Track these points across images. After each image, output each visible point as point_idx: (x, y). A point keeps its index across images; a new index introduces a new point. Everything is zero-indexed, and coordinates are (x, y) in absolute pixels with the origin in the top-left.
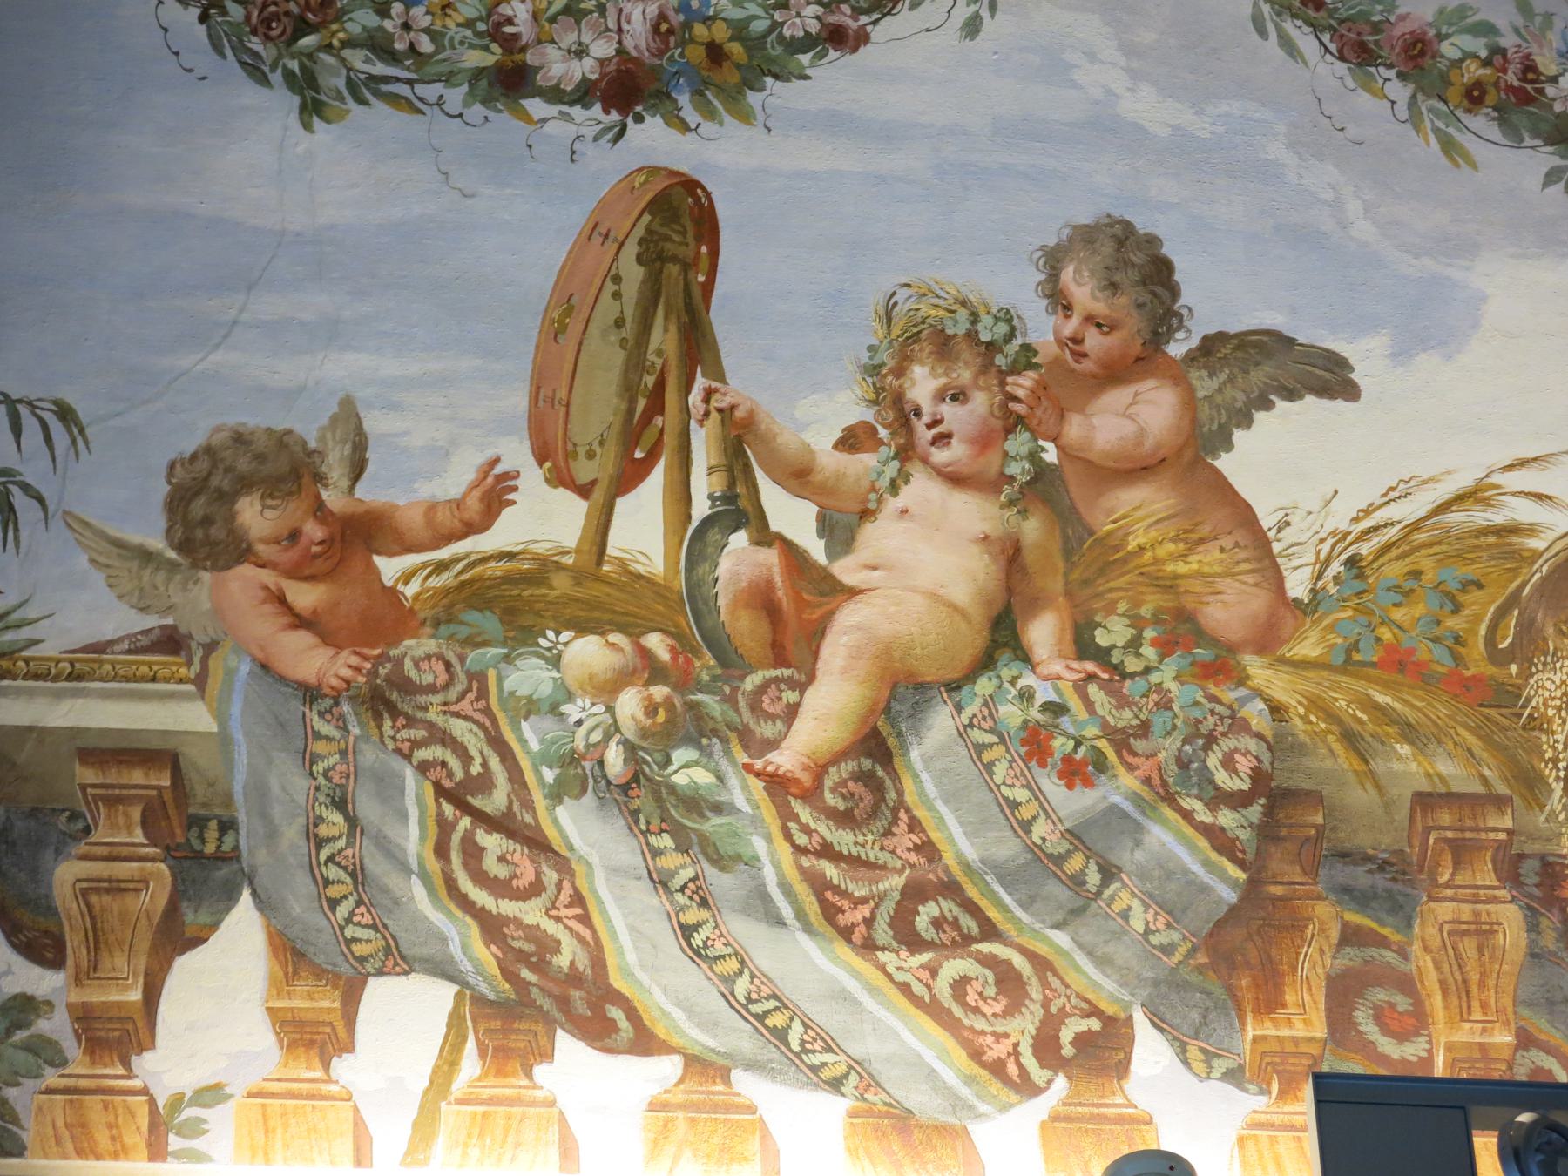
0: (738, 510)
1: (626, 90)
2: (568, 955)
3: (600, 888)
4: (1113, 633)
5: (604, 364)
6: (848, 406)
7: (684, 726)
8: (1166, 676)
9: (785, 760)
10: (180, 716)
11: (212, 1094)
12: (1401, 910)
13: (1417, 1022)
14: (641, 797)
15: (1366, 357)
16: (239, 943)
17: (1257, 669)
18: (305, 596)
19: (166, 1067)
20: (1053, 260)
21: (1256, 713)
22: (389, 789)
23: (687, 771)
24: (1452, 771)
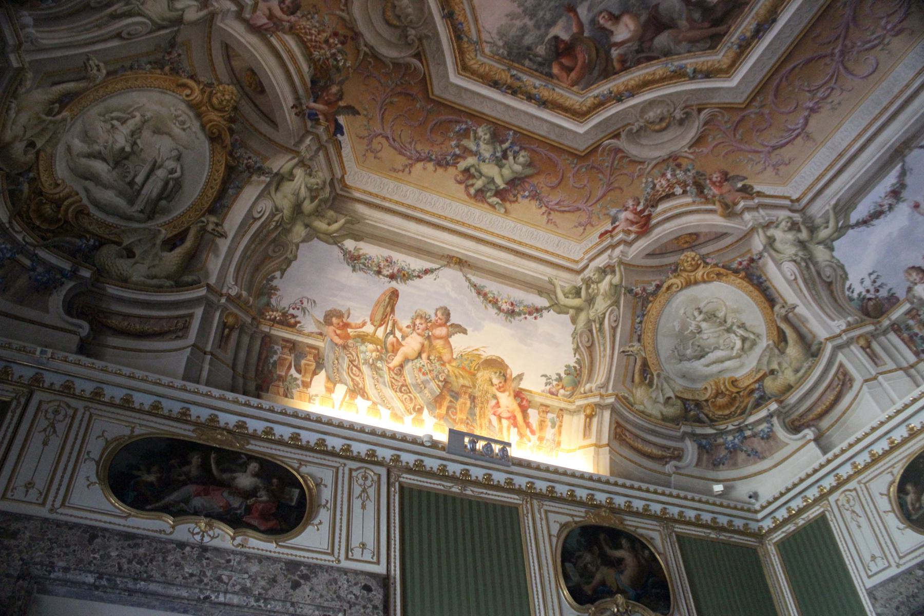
0: (392, 332)
1: (392, 277)
2: (361, 386)
3: (366, 378)
4: (432, 358)
5: (381, 310)
6: (409, 322)
7: (380, 359)
8: (437, 364)
9: (391, 365)
10: (320, 344)
11: (316, 395)
12: (457, 399)
13: (455, 414)
14: (373, 366)
15: (469, 330)
16: (322, 375)
17: (448, 366)
18: (338, 332)
19: (312, 390)
20: (437, 310)
21: (446, 371)
22: (343, 359)
23: (379, 364)
24: (467, 383)
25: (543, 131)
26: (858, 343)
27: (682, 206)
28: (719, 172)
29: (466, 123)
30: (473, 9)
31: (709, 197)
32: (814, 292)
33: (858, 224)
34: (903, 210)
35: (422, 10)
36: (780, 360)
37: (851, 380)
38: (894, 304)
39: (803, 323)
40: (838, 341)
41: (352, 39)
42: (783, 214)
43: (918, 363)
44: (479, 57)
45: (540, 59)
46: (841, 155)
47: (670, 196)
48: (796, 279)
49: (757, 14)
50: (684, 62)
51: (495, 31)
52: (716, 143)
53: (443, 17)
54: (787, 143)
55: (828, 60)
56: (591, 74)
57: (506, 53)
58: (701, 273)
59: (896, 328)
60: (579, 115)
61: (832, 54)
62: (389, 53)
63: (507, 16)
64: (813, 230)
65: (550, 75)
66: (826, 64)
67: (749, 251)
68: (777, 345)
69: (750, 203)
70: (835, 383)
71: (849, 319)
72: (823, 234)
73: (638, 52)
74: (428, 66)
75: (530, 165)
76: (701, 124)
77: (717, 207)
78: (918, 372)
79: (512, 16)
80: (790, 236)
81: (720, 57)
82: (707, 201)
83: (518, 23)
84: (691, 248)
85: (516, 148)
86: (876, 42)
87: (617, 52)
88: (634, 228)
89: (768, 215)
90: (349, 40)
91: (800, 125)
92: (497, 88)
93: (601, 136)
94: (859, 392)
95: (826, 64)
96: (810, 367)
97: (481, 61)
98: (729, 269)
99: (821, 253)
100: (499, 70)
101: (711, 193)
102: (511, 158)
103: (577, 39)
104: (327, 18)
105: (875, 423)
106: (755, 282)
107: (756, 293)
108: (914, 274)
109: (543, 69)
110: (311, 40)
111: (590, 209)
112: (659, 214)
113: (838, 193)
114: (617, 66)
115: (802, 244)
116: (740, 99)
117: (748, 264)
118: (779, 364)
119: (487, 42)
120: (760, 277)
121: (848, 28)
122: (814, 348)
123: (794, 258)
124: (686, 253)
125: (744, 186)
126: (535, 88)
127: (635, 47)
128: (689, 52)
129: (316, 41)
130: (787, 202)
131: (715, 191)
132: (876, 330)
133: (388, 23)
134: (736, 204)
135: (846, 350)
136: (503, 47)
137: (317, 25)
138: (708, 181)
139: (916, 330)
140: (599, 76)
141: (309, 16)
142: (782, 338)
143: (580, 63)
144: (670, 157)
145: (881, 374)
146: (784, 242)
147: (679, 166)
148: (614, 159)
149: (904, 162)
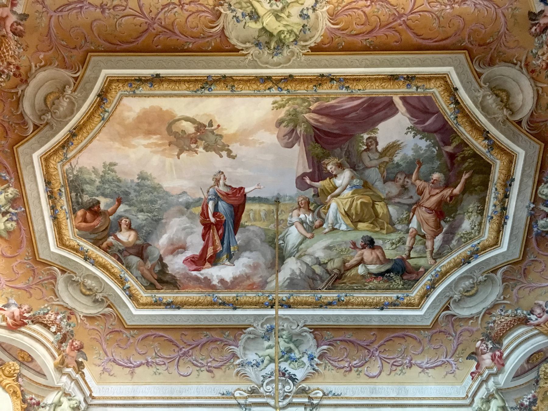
25: (37, 227)
27: (45, 338)
29: (11, 178)
30: (86, 146)
31: (62, 349)
35: (66, 117)
41: (21, 80)
44: (59, 165)
45: (80, 200)
46: (134, 398)
47: (46, 326)
49: (176, 297)
50: (130, 279)
51: (81, 166)
52: (96, 328)
53: (70, 131)
55: (177, 349)
56: (90, 234)
57: (72, 178)
58: (8, 382)
60: (61, 241)
61: (181, 349)
62: (26, 106)
63: (94, 168)
65: (74, 212)
67: (43, 397)
69: (74, 374)
73: (119, 251)
74: (33, 136)
75: (9, 232)
77: (58, 358)
79: (95, 171)
81: (144, 295)
82: (59, 350)
83: (93, 176)
84: (22, 364)
85: (15, 218)
86: (199, 365)
87: (112, 240)
88: (10, 321)
90: (19, 79)
91: (135, 364)
92: (46, 186)
93: (57, 263)
95: (174, 350)
97: (58, 169)
100: (58, 181)
101: (65, 348)
102: (6, 218)
103: (105, 214)
104: (24, 58)
109: (76, 206)
110: (4, 53)
111: (4, 286)
112: (30, 329)
114: (104, 245)
116: (130, 322)
117: (34, 404)
119: (71, 164)
121: (198, 346)
124: (15, 363)
125: (82, 362)
126: (61, 208)
127: (121, 248)
128: (137, 278)
129: (5, 57)
130: (88, 393)
131: (68, 349)
133: (45, 99)
134: (67, 367)
136: (74, 175)
137: (17, 53)
138: (71, 341)
140: (91, 239)
141: (19, 46)
143: (92, 224)
144: (70, 310)
147: (69, 318)
148: (48, 279)
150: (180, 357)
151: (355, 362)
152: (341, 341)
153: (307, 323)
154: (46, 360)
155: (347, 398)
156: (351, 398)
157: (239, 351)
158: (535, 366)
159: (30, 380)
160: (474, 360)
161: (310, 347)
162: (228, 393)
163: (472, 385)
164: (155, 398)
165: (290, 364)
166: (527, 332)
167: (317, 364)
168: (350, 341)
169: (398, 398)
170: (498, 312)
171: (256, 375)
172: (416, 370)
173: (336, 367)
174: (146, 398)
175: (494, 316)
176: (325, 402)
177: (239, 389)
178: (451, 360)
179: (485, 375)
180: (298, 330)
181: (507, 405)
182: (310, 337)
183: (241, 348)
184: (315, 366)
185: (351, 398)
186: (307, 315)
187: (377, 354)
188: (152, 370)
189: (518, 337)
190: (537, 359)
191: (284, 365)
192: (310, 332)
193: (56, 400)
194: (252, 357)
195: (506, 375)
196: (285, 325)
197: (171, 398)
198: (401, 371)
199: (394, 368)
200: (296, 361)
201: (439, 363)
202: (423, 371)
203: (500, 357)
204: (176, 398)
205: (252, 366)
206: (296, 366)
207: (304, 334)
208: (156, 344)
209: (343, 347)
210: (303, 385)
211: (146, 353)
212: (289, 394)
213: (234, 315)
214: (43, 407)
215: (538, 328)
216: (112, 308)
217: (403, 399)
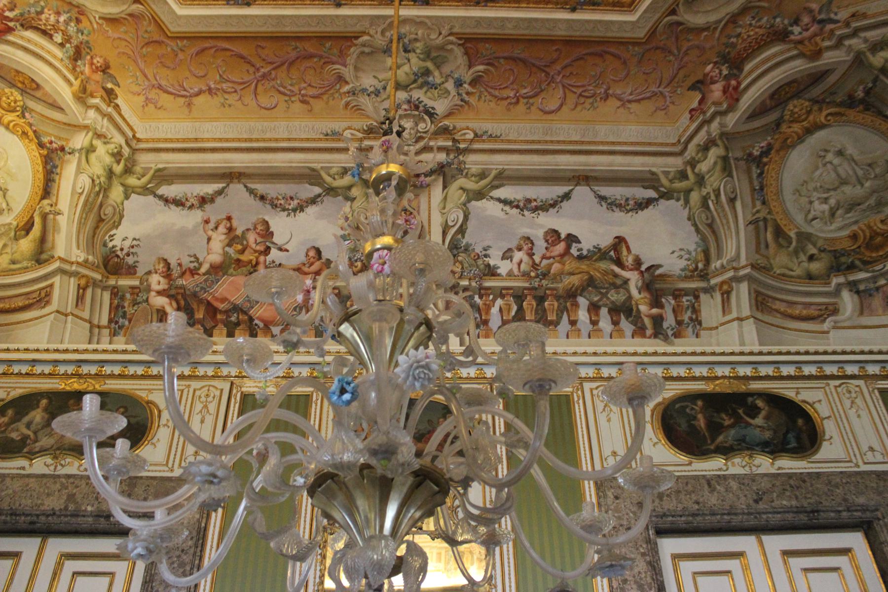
26: (79, 279)
27: (49, 52)
28: (105, 60)
31: (78, 70)
32: (84, 215)
33: (161, 197)
34: (197, 216)
36: (10, 243)
37: (48, 303)
38: (130, 274)
39: (54, 230)
40: (67, 267)
42: (119, 139)
43: (105, 327)
46: (196, 140)
48: (81, 194)
52: (123, 36)
54: (171, 93)
55: (252, 70)
59: (115, 292)
61: (258, 70)
64: (128, 171)
66: (248, 71)
67: (67, 140)
68: (17, 230)
69: (103, 106)
70: (34, 295)
71: (91, 258)
72: (132, 181)
76: (128, 11)
77: (77, 83)
78: (99, 334)
80: (108, 160)
82: (74, 70)
86: (288, 93)
89: (108, 129)
91: (192, 91)
94: (45, 316)
95: (248, 71)
96: (27, 268)
98: (37, 138)
99: (117, 193)
101: (82, 68)
105: (32, 346)
106: (49, 167)
107: (41, 176)
108: (162, 265)
113: (168, 163)
115: (110, 173)
116: (174, 28)
117: (56, 149)
118: (5, 246)
120: (56, 167)
121: (282, 64)
122: (44, 256)
123: (95, 178)
125: (112, 90)
130: (130, 134)
131: (87, 70)
132: (101, 281)
134: (92, 96)
135: (66, 278)
139: (126, 304)
142: (28, 227)
144: (78, 7)
145: (73, 315)
146: (99, 159)
147: (78, 21)
149: (228, 185)
150: (258, 81)
151: (525, 91)
152: (505, 58)
153: (455, 30)
154: (59, 85)
155: (509, 141)
156: (515, 142)
157: (347, 72)
158: (781, 104)
159: (43, 116)
160: (697, 92)
161: (458, 67)
162: (334, 133)
163: (688, 126)
164: (227, 140)
165: (426, 92)
166: (782, 53)
167: (468, 93)
168: (521, 60)
169: (582, 143)
170: (747, 20)
171: (375, 107)
172: (613, 103)
173: (496, 97)
174: (215, 140)
175: (740, 26)
176: (476, 146)
177: (349, 128)
178: (666, 92)
179: (708, 114)
180: (440, 41)
181: (730, 155)
182: (458, 52)
183: (351, 67)
184: (464, 95)
185: (515, 142)
186: (455, 17)
187: (558, 79)
188: (217, 100)
189: (768, 59)
190: (786, 93)
191: (417, 94)
192: (459, 45)
193: (86, 143)
194: (368, 81)
195: (738, 114)
196: (420, 32)
197: (251, 140)
198: (592, 104)
199: (582, 100)
200: (436, 88)
201: (648, 95)
202: (623, 105)
203: (736, 89)
204: (257, 140)
205: (369, 95)
206: (436, 95)
207: (450, 47)
208: (219, 61)
209: (508, 67)
210: (447, 122)
211: (204, 77)
212: (424, 135)
213: (337, 16)
214: (70, 153)
215: (800, 47)
216: (142, 4)
217: (589, 143)
